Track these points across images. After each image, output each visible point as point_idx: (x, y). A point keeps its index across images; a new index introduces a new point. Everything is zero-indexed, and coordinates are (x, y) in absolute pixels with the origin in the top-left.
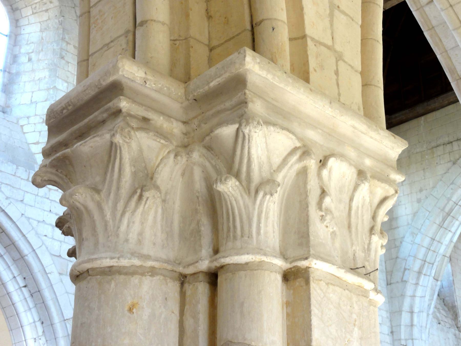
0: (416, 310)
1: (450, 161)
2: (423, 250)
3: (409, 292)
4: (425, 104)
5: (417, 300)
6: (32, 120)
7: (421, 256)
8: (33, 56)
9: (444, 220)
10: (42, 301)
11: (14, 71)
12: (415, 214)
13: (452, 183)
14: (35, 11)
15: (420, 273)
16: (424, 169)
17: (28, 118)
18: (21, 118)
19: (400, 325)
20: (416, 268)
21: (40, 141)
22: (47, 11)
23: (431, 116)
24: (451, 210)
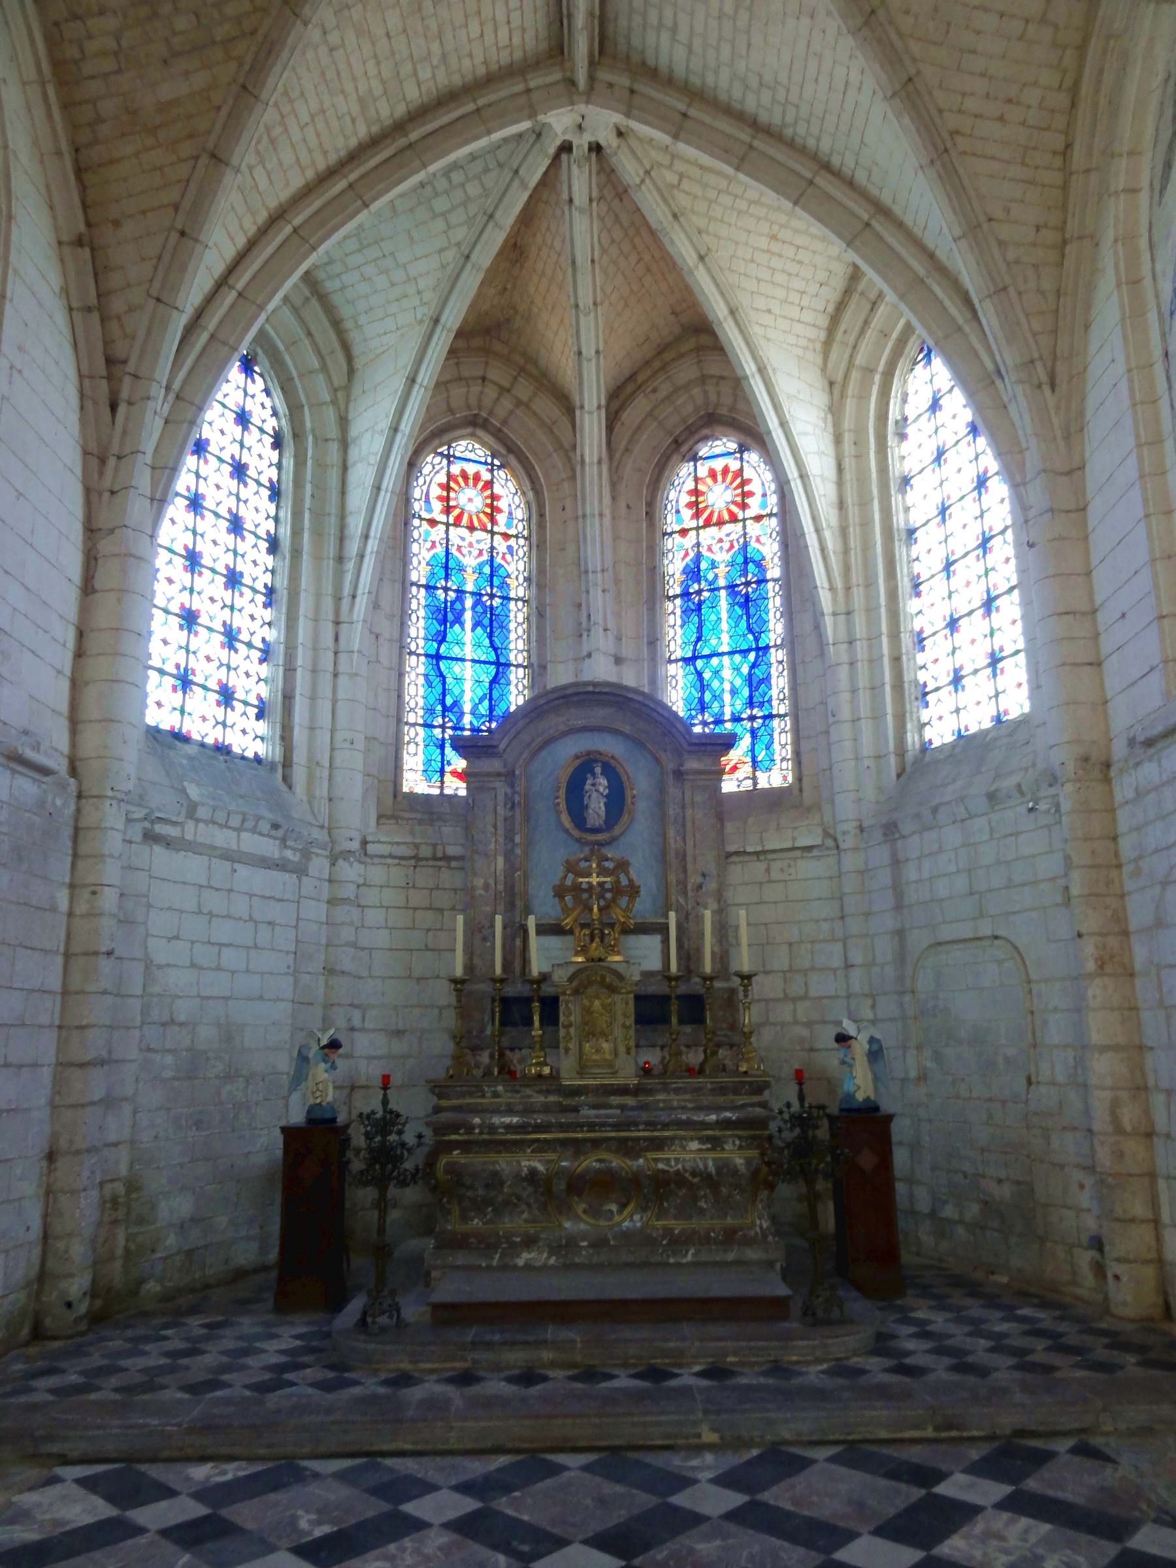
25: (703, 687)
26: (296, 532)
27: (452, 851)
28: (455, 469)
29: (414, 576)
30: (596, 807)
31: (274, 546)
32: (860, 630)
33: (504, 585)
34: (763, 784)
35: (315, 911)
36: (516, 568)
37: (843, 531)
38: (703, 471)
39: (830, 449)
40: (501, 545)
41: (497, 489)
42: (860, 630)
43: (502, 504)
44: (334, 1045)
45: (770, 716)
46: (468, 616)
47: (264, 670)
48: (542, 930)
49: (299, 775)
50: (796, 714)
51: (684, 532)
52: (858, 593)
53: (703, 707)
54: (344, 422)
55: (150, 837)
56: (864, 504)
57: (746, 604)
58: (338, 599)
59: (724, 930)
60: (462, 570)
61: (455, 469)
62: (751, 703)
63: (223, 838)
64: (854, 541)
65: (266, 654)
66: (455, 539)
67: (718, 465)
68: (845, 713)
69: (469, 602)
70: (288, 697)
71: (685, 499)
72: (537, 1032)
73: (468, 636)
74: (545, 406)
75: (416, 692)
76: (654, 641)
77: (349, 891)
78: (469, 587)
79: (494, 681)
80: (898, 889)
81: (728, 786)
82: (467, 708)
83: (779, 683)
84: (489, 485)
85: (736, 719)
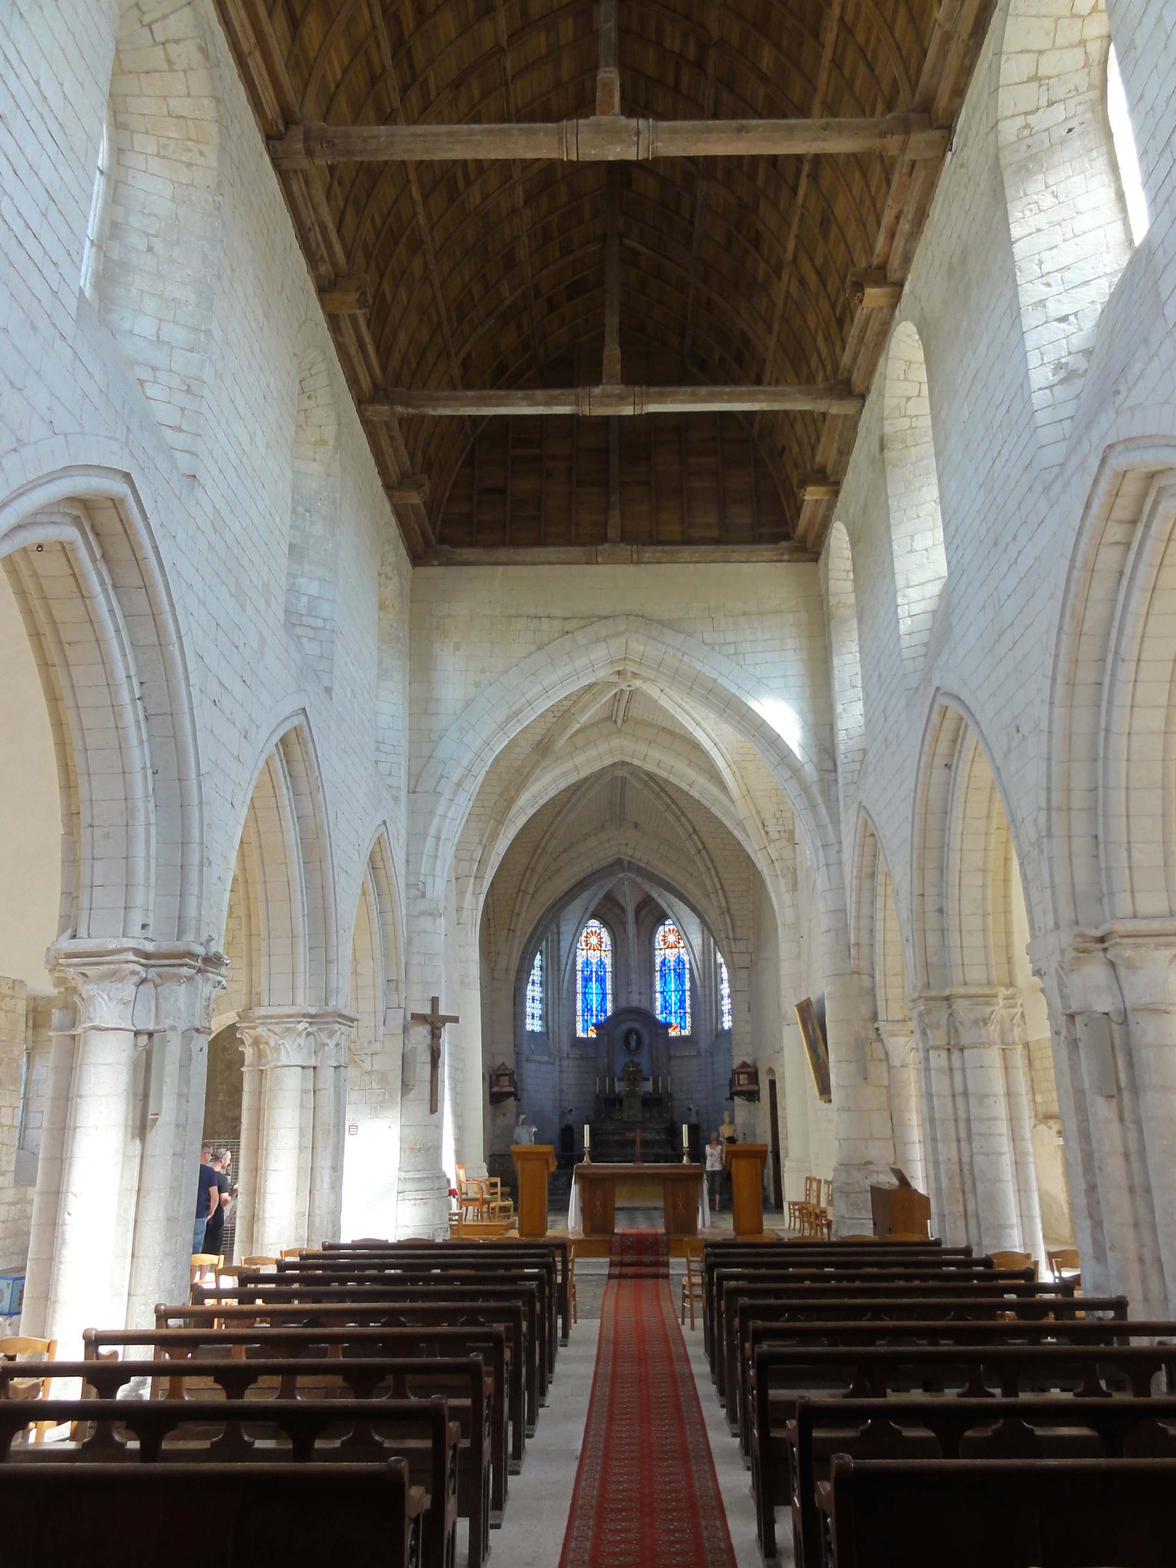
0: (443, 836)
1: (534, 643)
2: (469, 755)
3: (440, 810)
4: (512, 550)
5: (448, 821)
6: (163, 377)
7: (465, 762)
8: (158, 245)
9: (508, 720)
10: (171, 733)
11: (116, 257)
12: (468, 703)
13: (533, 674)
14: (163, 153)
15: (459, 785)
16: (492, 643)
17: (154, 369)
18: (138, 363)
19: (422, 854)
20: (455, 778)
21: (184, 427)
22: (189, 165)
23: (511, 568)
24: (521, 710)
25: (666, 1002)
26: (547, 962)
27: (593, 1055)
28: (589, 930)
29: (578, 968)
30: (633, 1044)
31: (541, 968)
32: (707, 993)
33: (605, 968)
34: (683, 1033)
35: (557, 1074)
36: (608, 961)
37: (704, 960)
38: (667, 929)
39: (700, 935)
40: (603, 954)
41: (602, 935)
42: (707, 993)
43: (603, 940)
44: (571, 1110)
45: (685, 1013)
46: (594, 979)
47: (540, 1006)
48: (618, 1080)
49: (551, 1035)
50: (693, 1015)
51: (661, 949)
52: (707, 981)
53: (666, 1008)
54: (558, 927)
55: (527, 1060)
56: (709, 953)
57: (680, 976)
58: (559, 982)
59: (665, 1081)
60: (591, 964)
61: (589, 930)
62: (680, 1008)
63: (538, 1058)
64: (707, 965)
65: (541, 1001)
66: (589, 955)
67: (672, 927)
68: (703, 1017)
69: (594, 974)
70: (547, 1012)
71: (661, 938)
72: (617, 1107)
73: (594, 986)
74: (618, 911)
75: (579, 1005)
76: (652, 985)
77: (564, 1069)
78: (594, 969)
79: (602, 1000)
80: (713, 1068)
81: (673, 1033)
82: (594, 1009)
83: (688, 1002)
84: (599, 934)
85: (676, 1013)
